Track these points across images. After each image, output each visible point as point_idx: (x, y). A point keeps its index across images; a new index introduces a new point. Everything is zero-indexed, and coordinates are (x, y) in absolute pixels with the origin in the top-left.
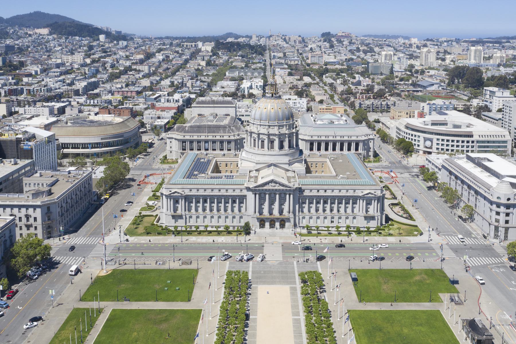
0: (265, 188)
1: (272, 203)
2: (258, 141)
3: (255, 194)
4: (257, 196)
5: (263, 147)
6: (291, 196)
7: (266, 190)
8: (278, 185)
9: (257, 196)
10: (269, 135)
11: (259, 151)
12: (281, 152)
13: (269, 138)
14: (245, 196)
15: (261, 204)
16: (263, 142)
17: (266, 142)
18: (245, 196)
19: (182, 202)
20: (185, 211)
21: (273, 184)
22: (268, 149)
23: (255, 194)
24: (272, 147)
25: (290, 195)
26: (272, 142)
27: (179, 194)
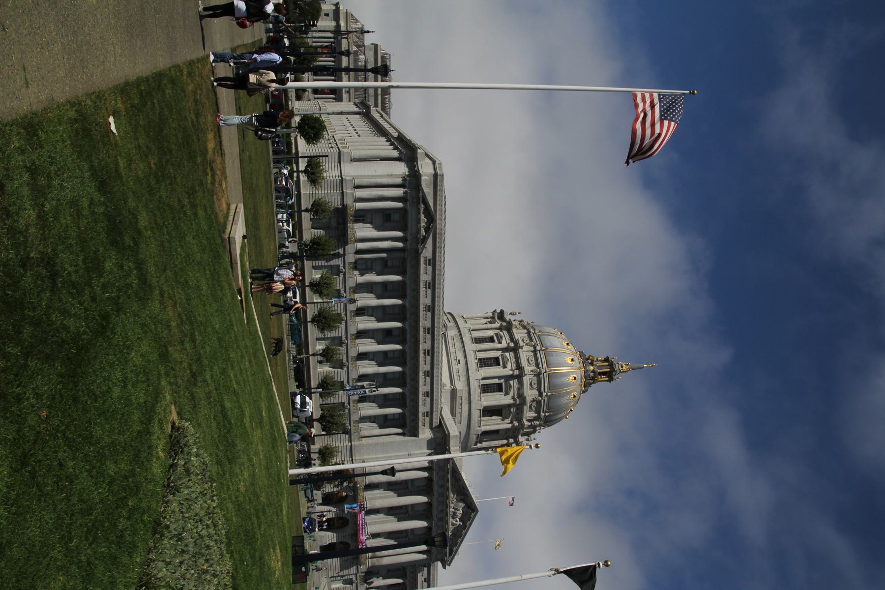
5: (484, 363)
16: (495, 362)
22: (484, 379)
24: (486, 389)
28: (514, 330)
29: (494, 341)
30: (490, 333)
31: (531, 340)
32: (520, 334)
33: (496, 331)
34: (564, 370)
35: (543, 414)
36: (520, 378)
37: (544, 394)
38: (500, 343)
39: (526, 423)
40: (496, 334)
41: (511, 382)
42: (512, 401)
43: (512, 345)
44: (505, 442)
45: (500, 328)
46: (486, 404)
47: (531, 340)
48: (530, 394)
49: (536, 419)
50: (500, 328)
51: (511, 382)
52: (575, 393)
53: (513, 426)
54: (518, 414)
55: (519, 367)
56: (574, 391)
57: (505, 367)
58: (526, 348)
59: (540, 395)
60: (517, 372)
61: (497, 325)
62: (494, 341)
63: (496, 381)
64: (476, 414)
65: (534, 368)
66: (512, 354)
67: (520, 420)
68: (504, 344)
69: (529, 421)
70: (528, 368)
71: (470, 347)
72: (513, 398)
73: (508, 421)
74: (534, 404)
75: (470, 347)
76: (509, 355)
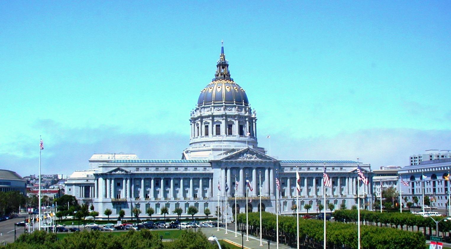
2: (213, 126)
4: (229, 171)
5: (218, 133)
7: (240, 162)
8: (255, 156)
9: (229, 171)
10: (226, 116)
12: (241, 138)
14: (212, 174)
16: (218, 126)
19: (126, 184)
20: (131, 197)
22: (226, 134)
24: (230, 133)
26: (229, 126)
27: (123, 172)
29: (208, 126)
30: (203, 126)
37: (235, 104)
38: (209, 123)
40: (204, 124)
42: (237, 121)
43: (211, 118)
45: (202, 121)
47: (209, 107)
48: (234, 112)
49: (245, 110)
50: (202, 121)
51: (229, 120)
55: (222, 116)
56: (234, 88)
58: (212, 112)
59: (235, 106)
62: (208, 126)
64: (242, 138)
65: (222, 108)
66: (215, 118)
67: (246, 117)
68: (210, 122)
69: (246, 113)
70: (222, 112)
71: (210, 138)
76: (216, 119)
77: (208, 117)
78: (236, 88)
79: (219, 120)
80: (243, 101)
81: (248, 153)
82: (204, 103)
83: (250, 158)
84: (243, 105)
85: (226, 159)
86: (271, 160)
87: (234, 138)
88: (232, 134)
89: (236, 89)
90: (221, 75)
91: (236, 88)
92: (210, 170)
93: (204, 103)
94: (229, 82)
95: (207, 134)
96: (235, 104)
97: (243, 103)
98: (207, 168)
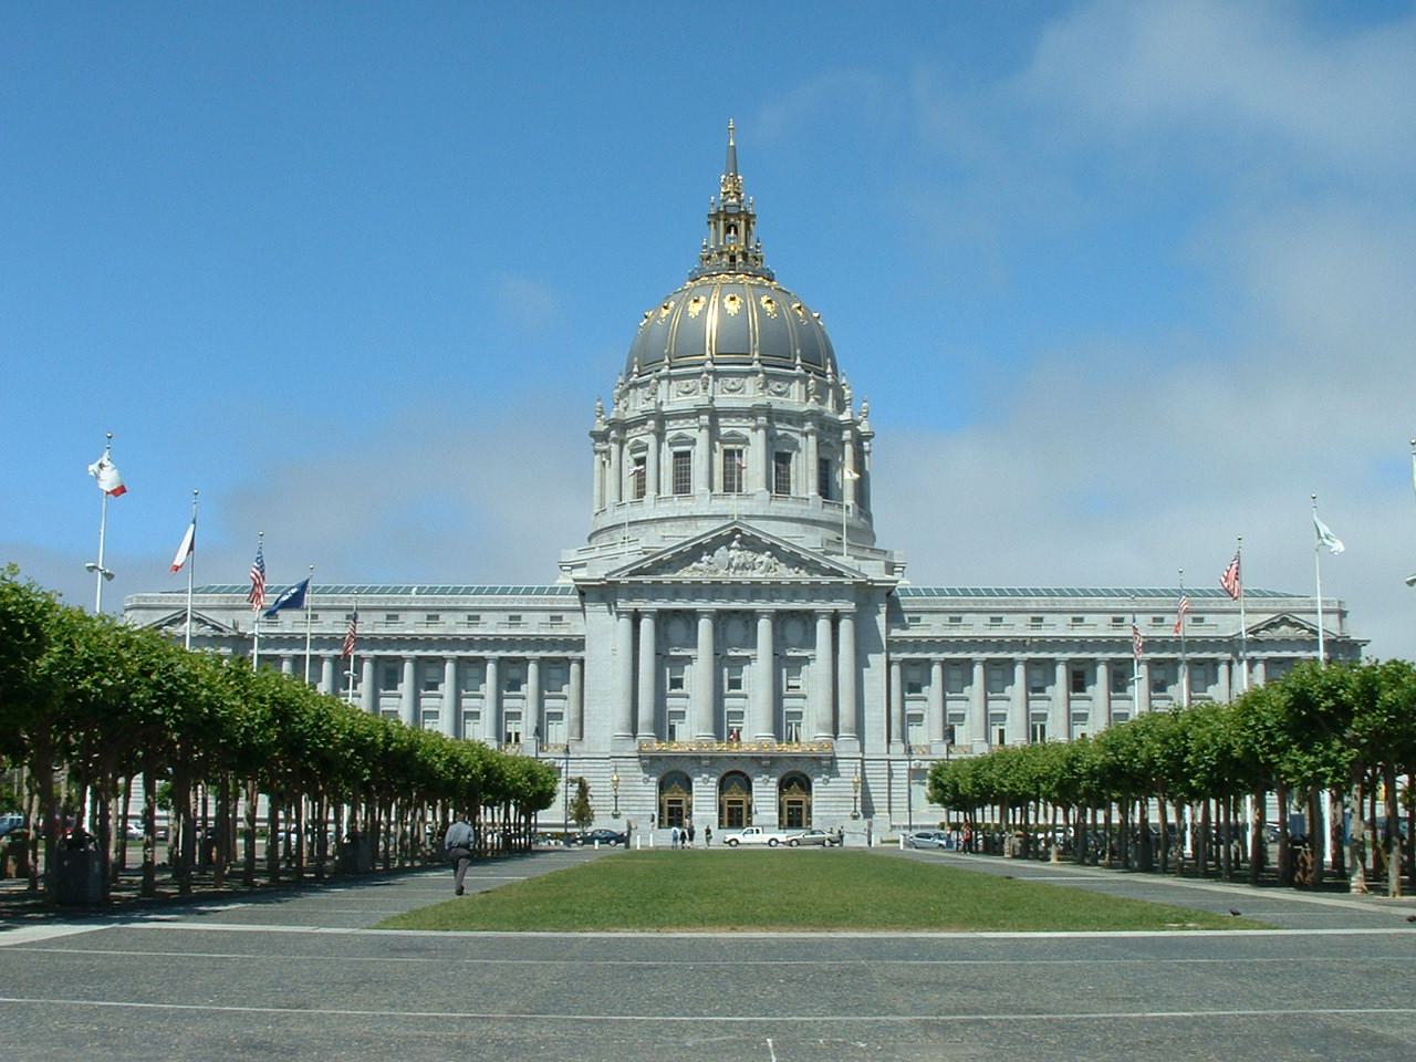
0: (686, 575)
1: (727, 672)
3: (636, 618)
4: (647, 625)
5: (682, 485)
6: (846, 627)
7: (697, 590)
8: (764, 558)
9: (647, 625)
11: (662, 505)
13: (713, 430)
15: (669, 666)
16: (682, 458)
17: (699, 454)
18: (579, 644)
21: (735, 554)
22: (711, 488)
23: (636, 618)
24: (732, 483)
25: (835, 619)
28: (628, 415)
31: (647, 383)
32: (638, 404)
33: (626, 451)
34: (712, 321)
35: (799, 370)
36: (715, 414)
37: (756, 366)
38: (646, 448)
39: (811, 405)
40: (633, 452)
41: (723, 431)
42: (761, 432)
44: (848, 448)
45: (622, 443)
46: (761, 487)
47: (647, 383)
48: (751, 393)
50: (622, 443)
52: (764, 299)
53: (812, 432)
54: (790, 423)
56: (758, 300)
57: (693, 442)
59: (755, 373)
60: (705, 419)
61: (614, 448)
63: (719, 458)
66: (671, 424)
68: (651, 440)
69: (807, 399)
71: (649, 508)
72: (755, 429)
73: (801, 440)
74: (774, 385)
75: (649, 508)
77: (641, 422)
78: (769, 302)
79: (684, 431)
80: (798, 351)
81: (735, 544)
82: (636, 369)
83: (744, 567)
84: (799, 370)
85: (632, 574)
86: (840, 574)
87: (746, 503)
88: (740, 490)
89: (769, 306)
90: (721, 254)
91: (769, 302)
92: (573, 626)
93: (636, 369)
94: (747, 280)
95: (641, 493)
96: (756, 366)
97: (798, 361)
98: (566, 617)
